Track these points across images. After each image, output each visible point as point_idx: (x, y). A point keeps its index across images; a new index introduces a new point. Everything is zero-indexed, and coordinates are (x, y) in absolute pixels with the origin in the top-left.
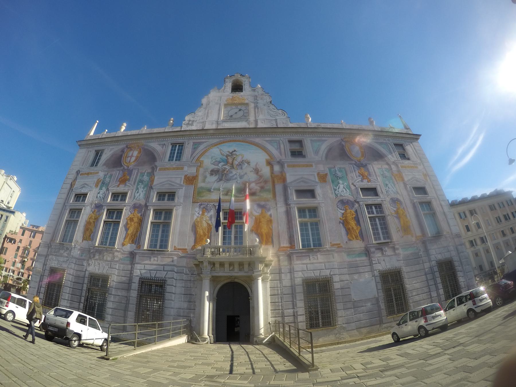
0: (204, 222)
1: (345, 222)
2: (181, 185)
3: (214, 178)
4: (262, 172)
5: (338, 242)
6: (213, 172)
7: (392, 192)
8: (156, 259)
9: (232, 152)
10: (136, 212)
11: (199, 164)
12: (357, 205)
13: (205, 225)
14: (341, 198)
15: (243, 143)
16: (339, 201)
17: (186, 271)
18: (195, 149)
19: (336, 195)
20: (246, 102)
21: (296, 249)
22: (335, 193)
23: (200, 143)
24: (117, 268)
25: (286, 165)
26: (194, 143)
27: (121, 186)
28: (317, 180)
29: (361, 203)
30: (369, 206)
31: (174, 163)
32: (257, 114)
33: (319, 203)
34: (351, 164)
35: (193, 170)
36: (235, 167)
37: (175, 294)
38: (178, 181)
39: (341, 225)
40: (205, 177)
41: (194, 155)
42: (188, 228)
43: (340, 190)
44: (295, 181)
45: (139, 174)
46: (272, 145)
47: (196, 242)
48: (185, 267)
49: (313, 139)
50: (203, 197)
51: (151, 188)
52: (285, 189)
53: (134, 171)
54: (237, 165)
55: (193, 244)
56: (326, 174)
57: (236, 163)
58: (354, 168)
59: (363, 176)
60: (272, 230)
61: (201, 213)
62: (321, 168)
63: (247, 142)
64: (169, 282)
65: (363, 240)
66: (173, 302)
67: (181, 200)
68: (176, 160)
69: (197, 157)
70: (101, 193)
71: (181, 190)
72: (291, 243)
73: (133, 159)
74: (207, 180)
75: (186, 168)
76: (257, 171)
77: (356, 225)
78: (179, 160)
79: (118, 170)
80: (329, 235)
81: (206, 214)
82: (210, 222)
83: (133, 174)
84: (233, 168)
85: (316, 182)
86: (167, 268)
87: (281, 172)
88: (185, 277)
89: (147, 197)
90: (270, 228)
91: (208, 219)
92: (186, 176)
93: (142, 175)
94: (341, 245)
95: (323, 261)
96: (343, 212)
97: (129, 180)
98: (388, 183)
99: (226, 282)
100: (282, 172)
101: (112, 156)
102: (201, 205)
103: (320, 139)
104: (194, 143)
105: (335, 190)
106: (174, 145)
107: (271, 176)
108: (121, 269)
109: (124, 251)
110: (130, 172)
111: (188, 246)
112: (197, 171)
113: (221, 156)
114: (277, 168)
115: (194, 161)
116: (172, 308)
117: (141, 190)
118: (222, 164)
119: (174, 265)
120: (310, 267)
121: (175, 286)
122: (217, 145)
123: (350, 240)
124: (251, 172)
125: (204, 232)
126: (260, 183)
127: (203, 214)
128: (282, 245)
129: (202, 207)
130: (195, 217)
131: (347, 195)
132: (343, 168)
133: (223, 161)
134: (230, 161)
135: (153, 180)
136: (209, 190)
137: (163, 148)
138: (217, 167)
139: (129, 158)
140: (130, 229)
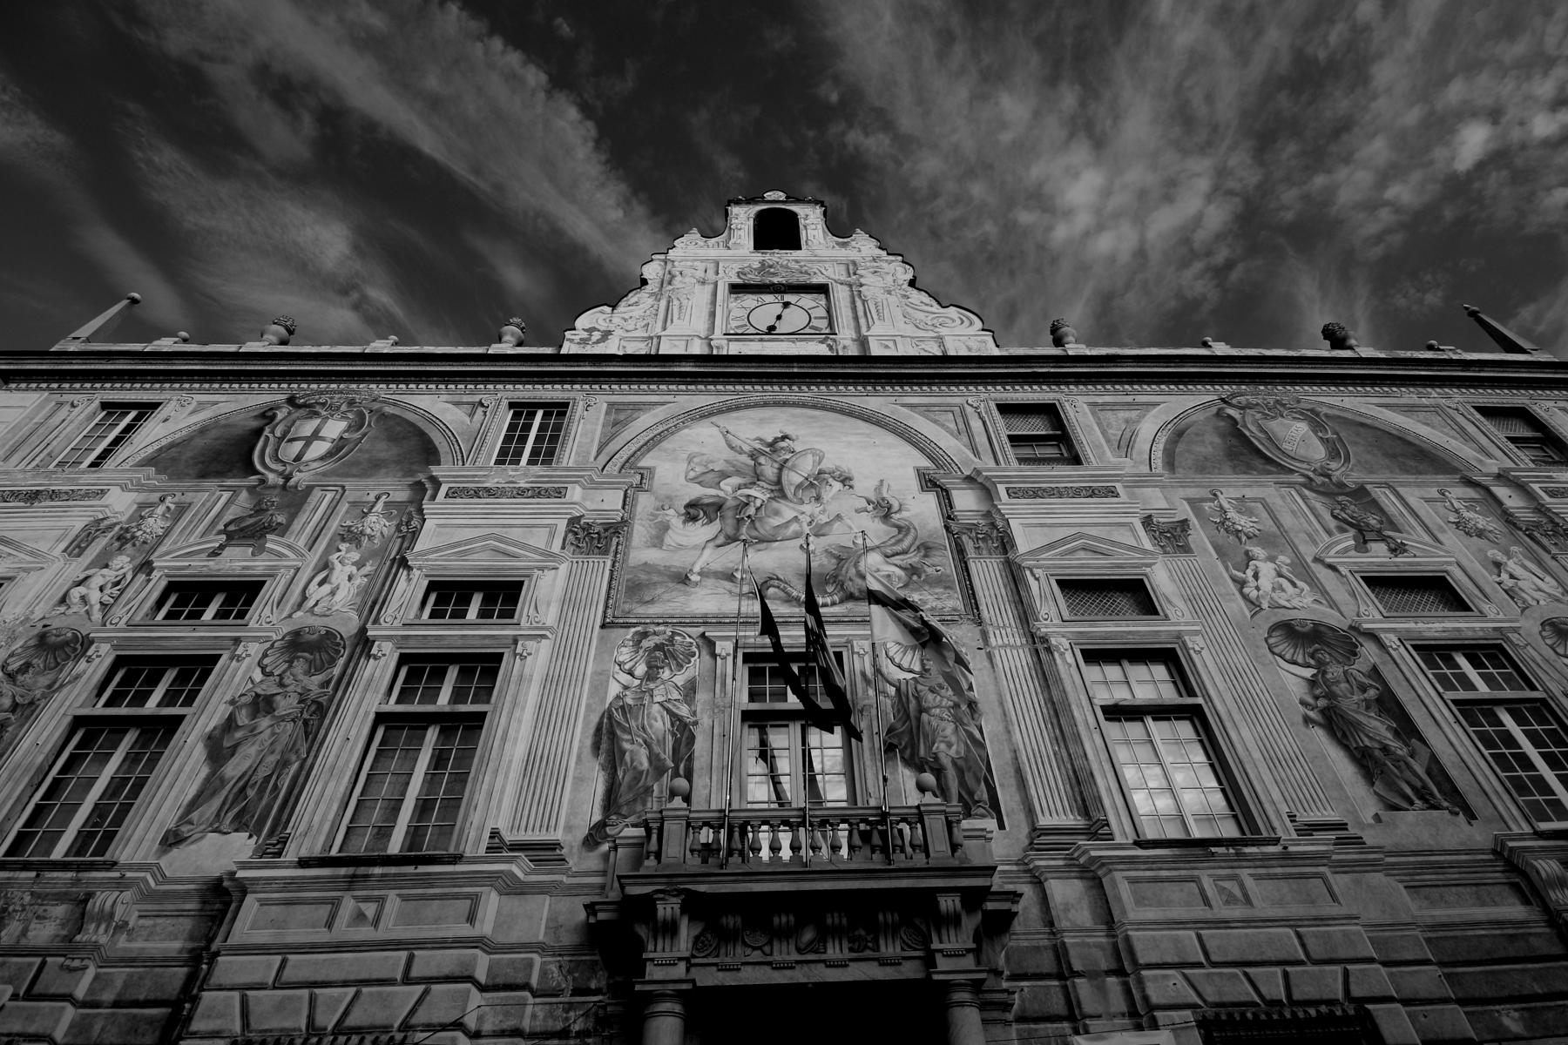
0: (656, 707)
1: (1335, 723)
2: (549, 555)
3: (702, 532)
4: (904, 514)
5: (1331, 816)
6: (694, 511)
7: (1538, 595)
8: (370, 910)
9: (776, 440)
10: (299, 667)
12: (1369, 651)
13: (659, 725)
15: (817, 413)
17: (544, 973)
19: (1254, 605)
20: (817, 280)
21: (1119, 839)
22: (1245, 597)
23: (638, 407)
24: (80, 993)
25: (1001, 488)
26: (611, 405)
27: (227, 552)
28: (1147, 544)
30: (1434, 653)
31: (524, 473)
32: (862, 321)
33: (1179, 636)
34: (1290, 485)
35: (610, 502)
36: (789, 491)
38: (538, 539)
39: (1319, 734)
40: (665, 528)
41: (612, 447)
42: (580, 735)
43: (1266, 582)
44: (1050, 546)
45: (344, 507)
46: (935, 422)
47: (611, 802)
48: (540, 948)
49: (1100, 400)
50: (652, 602)
51: (403, 563)
52: (1014, 576)
53: (317, 493)
54: (799, 486)
55: (597, 817)
56: (1184, 523)
57: (792, 479)
58: (1304, 498)
59: (1360, 531)
60: (981, 745)
61: (641, 669)
62: (1155, 499)
63: (833, 410)
65: (1471, 816)
67: (550, 617)
68: (530, 462)
69: (625, 454)
70: (97, 581)
71: (549, 574)
72: (1085, 811)
73: (319, 448)
74: (671, 538)
75: (575, 493)
76: (885, 510)
77: (1396, 733)
78: (547, 462)
79: (228, 489)
80: (1267, 777)
81: (666, 674)
82: (684, 711)
83: (308, 508)
84: (784, 497)
85: (1145, 552)
86: (427, 963)
87: (988, 514)
89: (373, 603)
90: (971, 735)
91: (676, 695)
92: (573, 521)
93: (362, 510)
94: (1353, 831)
95: (1279, 913)
97: (282, 530)
98: (1501, 557)
101: (203, 431)
102: (645, 635)
103: (1129, 399)
104: (611, 405)
105: (1241, 584)
106: (523, 410)
107: (947, 528)
108: (108, 996)
109: (166, 880)
110: (296, 499)
111: (569, 828)
113: (728, 454)
114: (966, 501)
115: (613, 468)
117: (340, 574)
118: (736, 480)
120: (1224, 943)
122: (711, 414)
123: (1396, 808)
124: (858, 511)
125: (653, 758)
126: (905, 552)
127: (651, 676)
128: (1044, 821)
129: (646, 643)
130: (614, 689)
131: (1302, 604)
132: (1254, 500)
133: (738, 473)
134: (769, 470)
135: (415, 535)
136: (683, 579)
137: (471, 415)
138: (712, 492)
139: (298, 445)
140: (241, 751)
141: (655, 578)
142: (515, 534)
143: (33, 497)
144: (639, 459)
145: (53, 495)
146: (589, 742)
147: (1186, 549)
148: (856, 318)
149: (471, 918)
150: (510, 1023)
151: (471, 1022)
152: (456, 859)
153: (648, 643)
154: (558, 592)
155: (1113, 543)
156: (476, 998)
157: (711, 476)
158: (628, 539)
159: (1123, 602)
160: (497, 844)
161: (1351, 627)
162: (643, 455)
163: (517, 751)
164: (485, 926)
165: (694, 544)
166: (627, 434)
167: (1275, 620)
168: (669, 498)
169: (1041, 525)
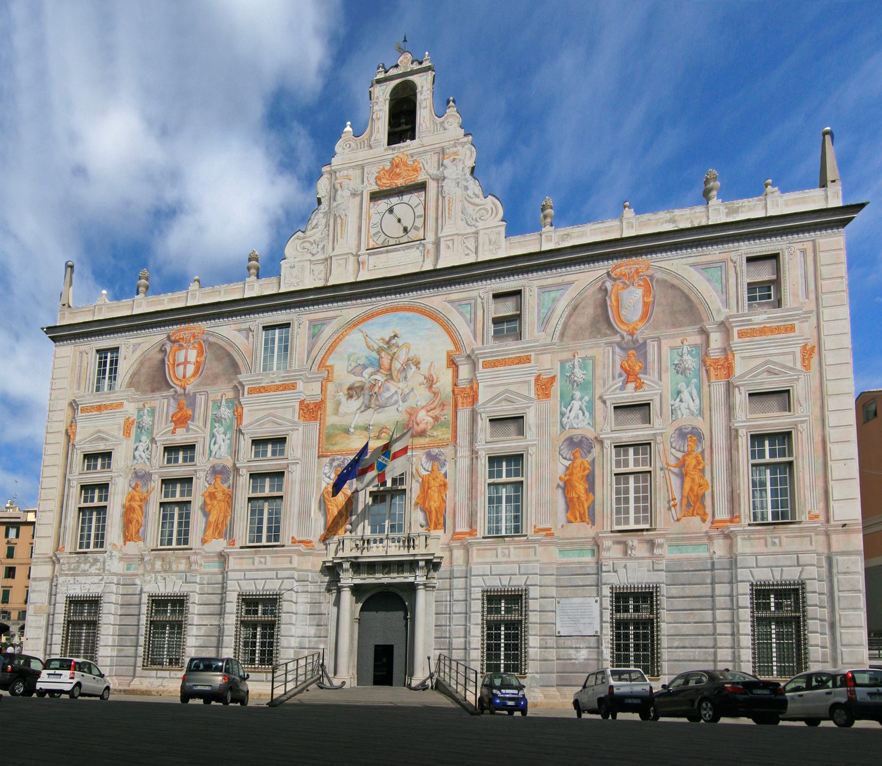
2: (294, 422)
11: (325, 374)
12: (596, 449)
14: (573, 432)
16: (564, 441)
17: (312, 577)
18: (314, 336)
19: (563, 426)
23: (324, 322)
28: (533, 395)
29: (607, 443)
37: (296, 614)
40: (339, 403)
41: (314, 354)
43: (573, 414)
44: (492, 399)
50: (335, 444)
64: (286, 596)
66: (293, 627)
67: (298, 454)
69: (319, 358)
74: (342, 409)
75: (300, 385)
86: (282, 574)
88: (311, 588)
92: (302, 402)
96: (567, 463)
99: (374, 592)
100: (473, 382)
102: (333, 460)
112: (323, 389)
115: (315, 368)
116: (292, 636)
119: (294, 569)
121: (296, 603)
130: (324, 485)
131: (581, 426)
141: (337, 432)
142: (279, 412)
143: (99, 408)
144: (326, 361)
145: (106, 407)
146: (317, 506)
147: (548, 396)
148: (437, 219)
149: (291, 562)
150: (305, 590)
151: (295, 589)
152: (283, 546)
153: (335, 464)
154: (300, 442)
155: (519, 395)
156: (296, 584)
157: (358, 368)
158: (325, 411)
159: (512, 427)
160: (294, 541)
161: (596, 438)
162: (328, 357)
163: (295, 510)
164: (295, 565)
165: (350, 412)
166: (320, 344)
167: (568, 435)
168: (340, 385)
169: (492, 386)
